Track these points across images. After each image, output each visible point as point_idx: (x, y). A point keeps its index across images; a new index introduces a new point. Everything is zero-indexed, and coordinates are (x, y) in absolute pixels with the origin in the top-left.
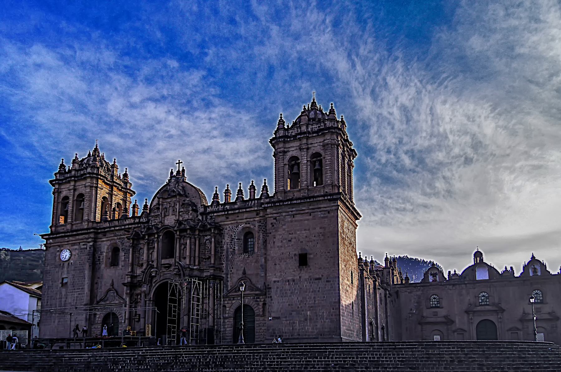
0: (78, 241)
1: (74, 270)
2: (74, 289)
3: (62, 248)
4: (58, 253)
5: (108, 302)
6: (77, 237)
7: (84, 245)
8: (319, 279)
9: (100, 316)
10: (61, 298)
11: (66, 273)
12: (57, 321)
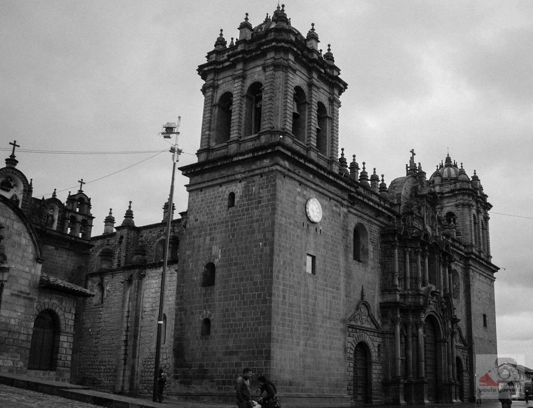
0: (331, 195)
1: (324, 247)
2: (326, 286)
3: (305, 192)
4: (298, 198)
5: (359, 324)
6: (327, 186)
7: (336, 206)
8: (491, 341)
9: (351, 342)
10: (308, 298)
11: (313, 245)
12: (302, 342)
